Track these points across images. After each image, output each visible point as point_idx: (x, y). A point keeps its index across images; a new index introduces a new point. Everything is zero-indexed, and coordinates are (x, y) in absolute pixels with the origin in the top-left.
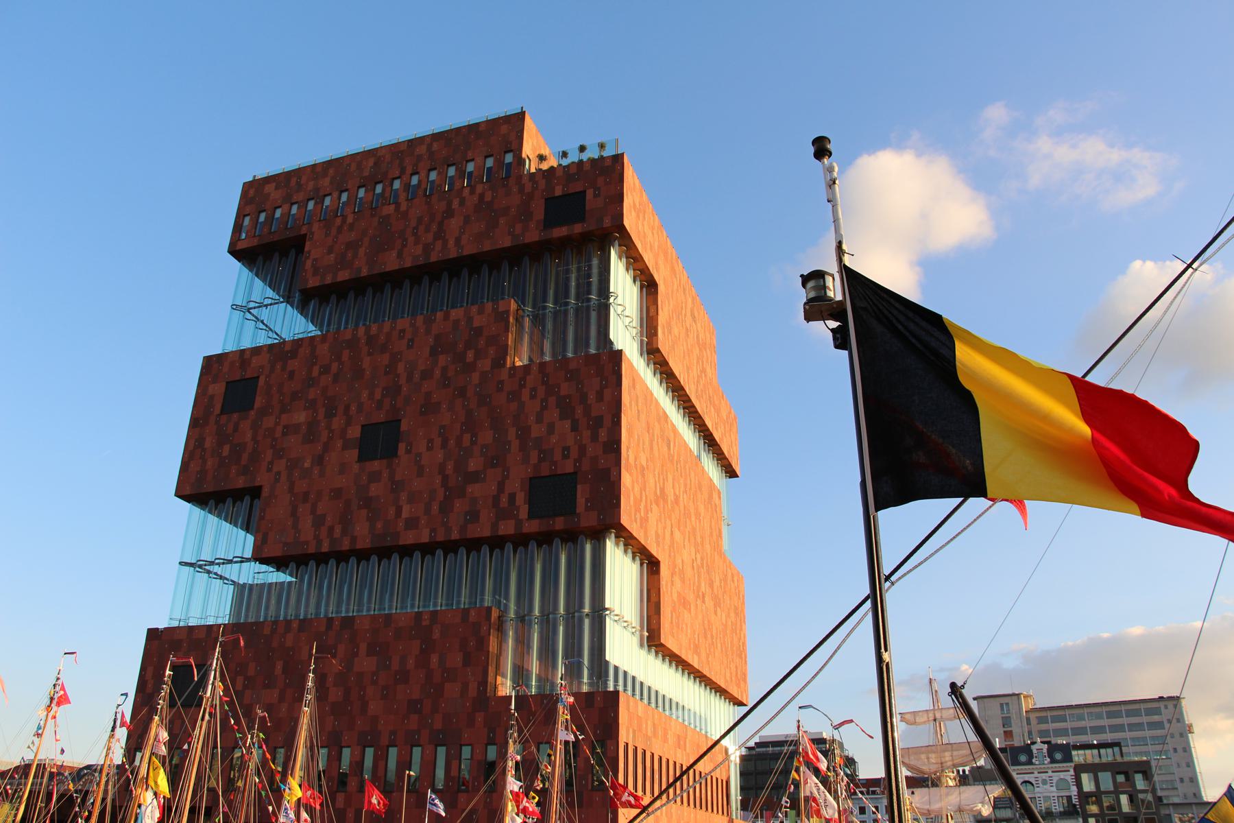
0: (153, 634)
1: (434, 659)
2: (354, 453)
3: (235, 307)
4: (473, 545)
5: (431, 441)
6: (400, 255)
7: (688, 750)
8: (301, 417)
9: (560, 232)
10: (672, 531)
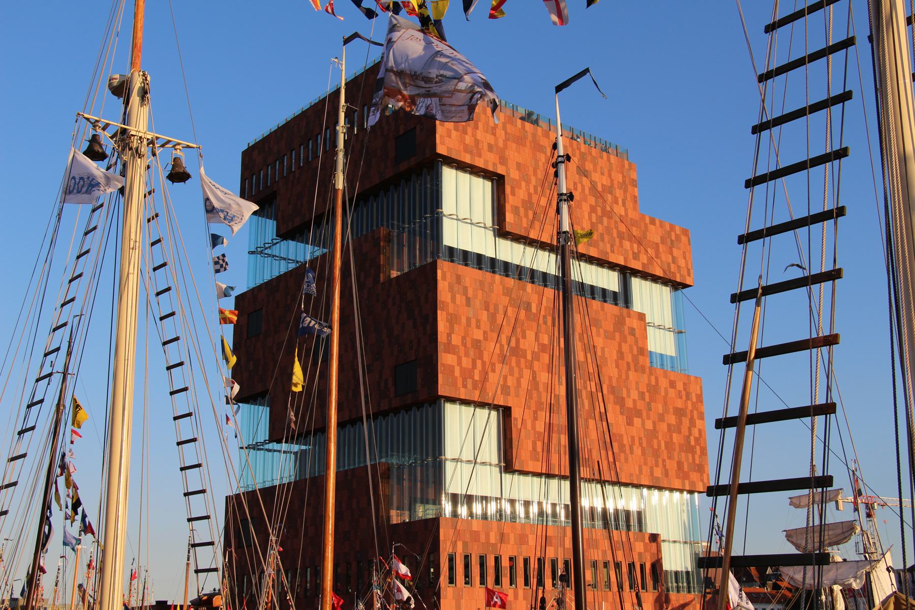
9: (403, 166)
10: (534, 378)
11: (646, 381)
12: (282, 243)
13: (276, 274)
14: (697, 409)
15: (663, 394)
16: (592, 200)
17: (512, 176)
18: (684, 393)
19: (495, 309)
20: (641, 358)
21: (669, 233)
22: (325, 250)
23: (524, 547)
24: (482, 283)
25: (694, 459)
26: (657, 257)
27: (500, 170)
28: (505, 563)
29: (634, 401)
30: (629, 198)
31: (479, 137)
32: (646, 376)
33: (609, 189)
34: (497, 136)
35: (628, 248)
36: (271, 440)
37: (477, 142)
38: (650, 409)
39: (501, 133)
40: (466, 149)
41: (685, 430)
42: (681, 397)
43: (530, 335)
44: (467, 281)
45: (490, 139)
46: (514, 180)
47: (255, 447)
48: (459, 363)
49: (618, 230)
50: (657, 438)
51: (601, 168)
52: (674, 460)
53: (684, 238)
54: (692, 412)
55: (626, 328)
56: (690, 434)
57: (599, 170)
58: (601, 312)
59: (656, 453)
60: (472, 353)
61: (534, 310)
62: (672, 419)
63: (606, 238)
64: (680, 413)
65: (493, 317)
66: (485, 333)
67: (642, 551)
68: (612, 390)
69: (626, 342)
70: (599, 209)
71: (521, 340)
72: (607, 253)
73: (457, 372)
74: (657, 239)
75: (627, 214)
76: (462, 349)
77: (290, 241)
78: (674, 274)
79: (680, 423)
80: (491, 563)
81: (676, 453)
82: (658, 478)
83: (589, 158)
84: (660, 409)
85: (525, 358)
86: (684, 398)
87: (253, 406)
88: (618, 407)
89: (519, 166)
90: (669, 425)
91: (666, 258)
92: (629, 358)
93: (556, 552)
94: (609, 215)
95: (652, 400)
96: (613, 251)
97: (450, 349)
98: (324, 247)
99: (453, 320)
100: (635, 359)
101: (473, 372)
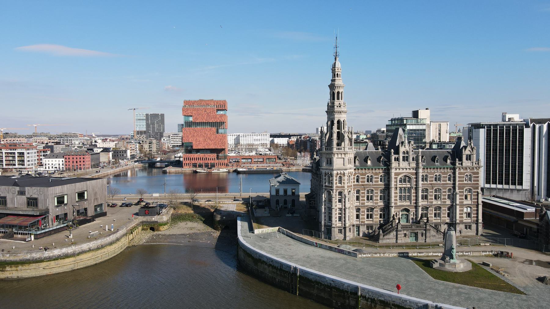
20: (214, 133)
28: (191, 158)
33: (210, 112)
40: (187, 114)
41: (221, 141)
43: (196, 134)
45: (190, 111)
53: (224, 116)
62: (219, 140)
63: (209, 119)
64: (221, 139)
65: (190, 133)
68: (209, 138)
80: (190, 158)
84: (217, 139)
89: (194, 114)
91: (220, 119)
92: (212, 134)
100: (213, 134)
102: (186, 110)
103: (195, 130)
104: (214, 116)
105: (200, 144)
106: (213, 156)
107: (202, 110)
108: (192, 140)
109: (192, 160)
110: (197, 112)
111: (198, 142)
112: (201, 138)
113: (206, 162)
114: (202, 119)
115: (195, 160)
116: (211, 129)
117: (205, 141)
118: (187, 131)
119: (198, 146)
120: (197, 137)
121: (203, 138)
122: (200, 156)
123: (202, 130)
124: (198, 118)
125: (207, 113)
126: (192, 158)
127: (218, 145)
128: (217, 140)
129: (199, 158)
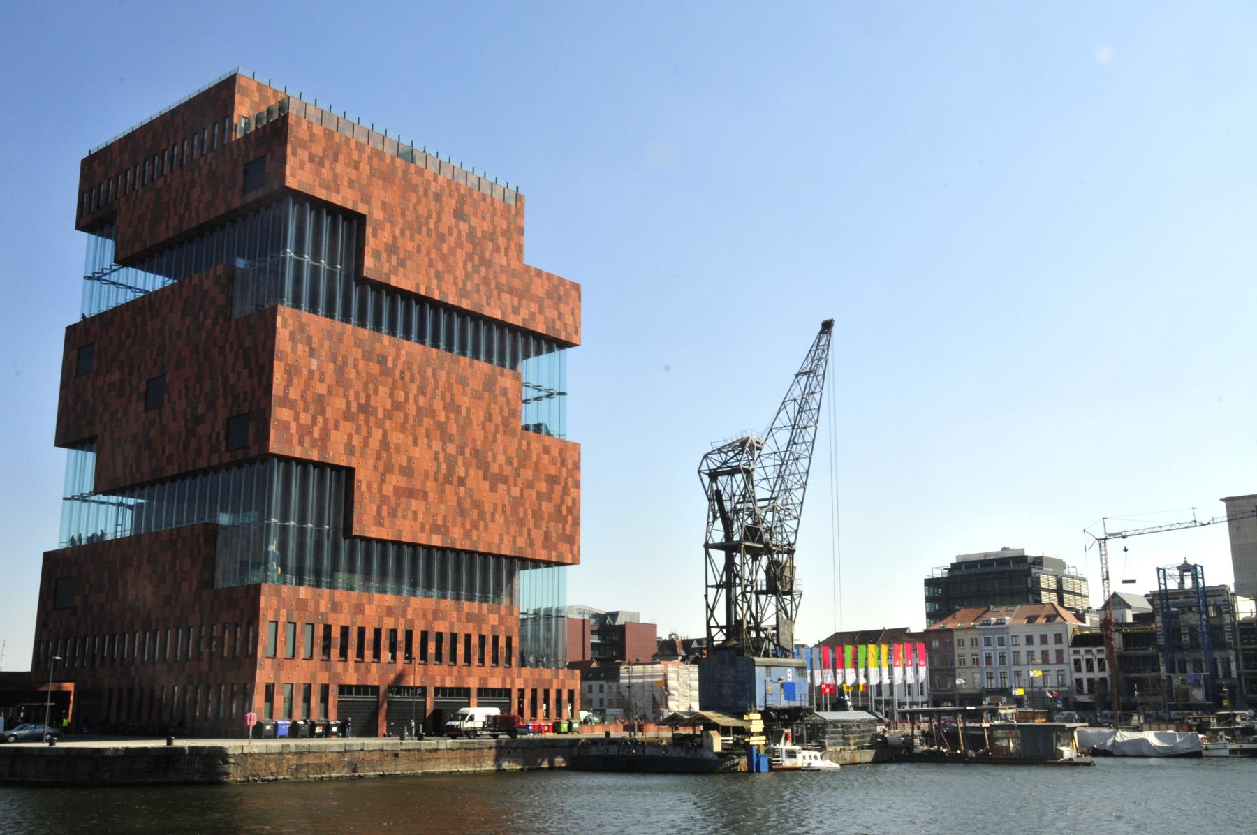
0: (48, 556)
1: (178, 564)
2: (142, 404)
3: (85, 278)
4: (205, 472)
5: (180, 391)
6: (167, 228)
7: (409, 617)
8: (116, 376)
9: (251, 197)
10: (384, 437)
11: (516, 445)
12: (122, 270)
13: (121, 301)
14: (573, 477)
15: (534, 459)
16: (468, 247)
17: (375, 216)
18: (559, 460)
19: (343, 362)
20: (512, 421)
21: (557, 287)
22: (176, 281)
23: (359, 617)
24: (330, 335)
25: (564, 529)
26: (540, 312)
27: (362, 209)
28: (336, 633)
29: (500, 466)
30: (513, 246)
31: (338, 171)
32: (516, 440)
33: (491, 236)
34: (361, 170)
35: (508, 302)
36: (96, 491)
37: (335, 176)
38: (518, 475)
39: (365, 168)
41: (556, 497)
42: (554, 463)
43: (384, 391)
44: (313, 331)
45: (353, 174)
46: (376, 221)
47: (82, 498)
48: (297, 418)
49: (497, 281)
50: (523, 505)
51: (483, 212)
52: (541, 529)
53: (573, 293)
54: (566, 479)
55: (497, 388)
56: (563, 501)
57: (480, 215)
58: (469, 370)
59: (521, 523)
60: (312, 407)
61: (390, 364)
62: (543, 487)
63: (482, 288)
64: (552, 480)
65: (340, 371)
66: (329, 386)
67: (496, 623)
68: (476, 453)
69: (496, 403)
70: (476, 257)
71: (373, 397)
72: (482, 306)
73: (293, 426)
74: (541, 292)
75: (508, 263)
76: (301, 405)
77: (130, 269)
78: (559, 331)
79: (551, 491)
81: (544, 524)
82: (521, 548)
83: (469, 201)
85: (376, 416)
86: (559, 465)
87: (80, 452)
88: (481, 472)
89: (384, 206)
90: (538, 493)
91: (551, 313)
92: (497, 419)
93: (397, 622)
94: (488, 264)
95: (522, 464)
96: (488, 304)
97: (286, 402)
98: (175, 279)
99: (291, 372)
100: (505, 423)
101: (313, 429)
102: (318, 150)
103: (382, 360)
104: (514, 273)
105: (411, 493)
106: (502, 620)
107: (438, 197)
108: (350, 450)
109: (344, 653)
110: (404, 197)
111: (395, 480)
112: (423, 440)
113: (449, 683)
114: (439, 276)
115: (368, 653)
116: (489, 385)
117: (448, 480)
118: (312, 352)
119: (393, 514)
120: (388, 424)
121: (437, 445)
122: (404, 615)
123: (435, 375)
124: (409, 255)
125: (471, 234)
126: (345, 631)
127: (537, 527)
128: (530, 485)
129: (401, 637)
